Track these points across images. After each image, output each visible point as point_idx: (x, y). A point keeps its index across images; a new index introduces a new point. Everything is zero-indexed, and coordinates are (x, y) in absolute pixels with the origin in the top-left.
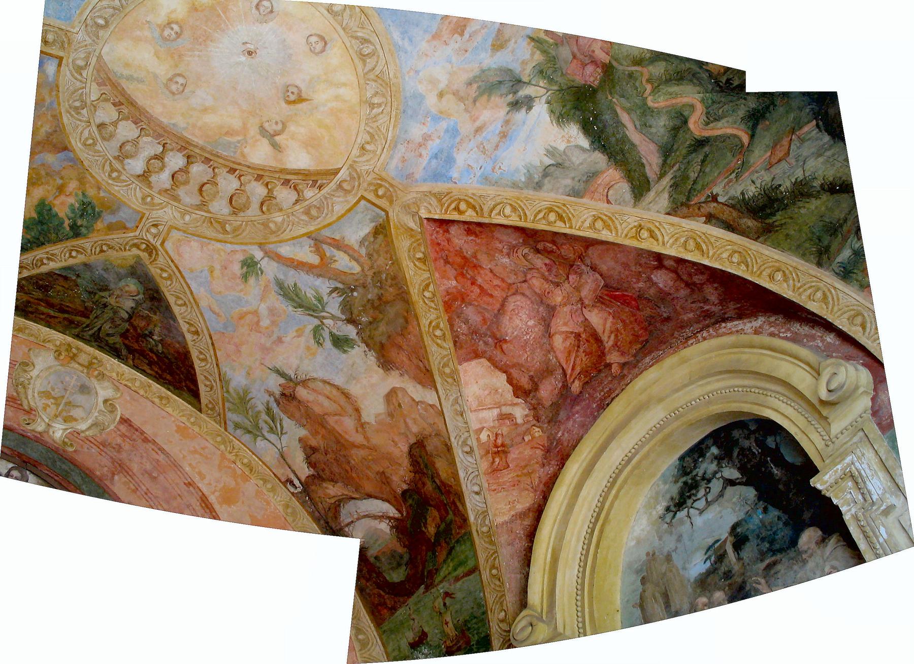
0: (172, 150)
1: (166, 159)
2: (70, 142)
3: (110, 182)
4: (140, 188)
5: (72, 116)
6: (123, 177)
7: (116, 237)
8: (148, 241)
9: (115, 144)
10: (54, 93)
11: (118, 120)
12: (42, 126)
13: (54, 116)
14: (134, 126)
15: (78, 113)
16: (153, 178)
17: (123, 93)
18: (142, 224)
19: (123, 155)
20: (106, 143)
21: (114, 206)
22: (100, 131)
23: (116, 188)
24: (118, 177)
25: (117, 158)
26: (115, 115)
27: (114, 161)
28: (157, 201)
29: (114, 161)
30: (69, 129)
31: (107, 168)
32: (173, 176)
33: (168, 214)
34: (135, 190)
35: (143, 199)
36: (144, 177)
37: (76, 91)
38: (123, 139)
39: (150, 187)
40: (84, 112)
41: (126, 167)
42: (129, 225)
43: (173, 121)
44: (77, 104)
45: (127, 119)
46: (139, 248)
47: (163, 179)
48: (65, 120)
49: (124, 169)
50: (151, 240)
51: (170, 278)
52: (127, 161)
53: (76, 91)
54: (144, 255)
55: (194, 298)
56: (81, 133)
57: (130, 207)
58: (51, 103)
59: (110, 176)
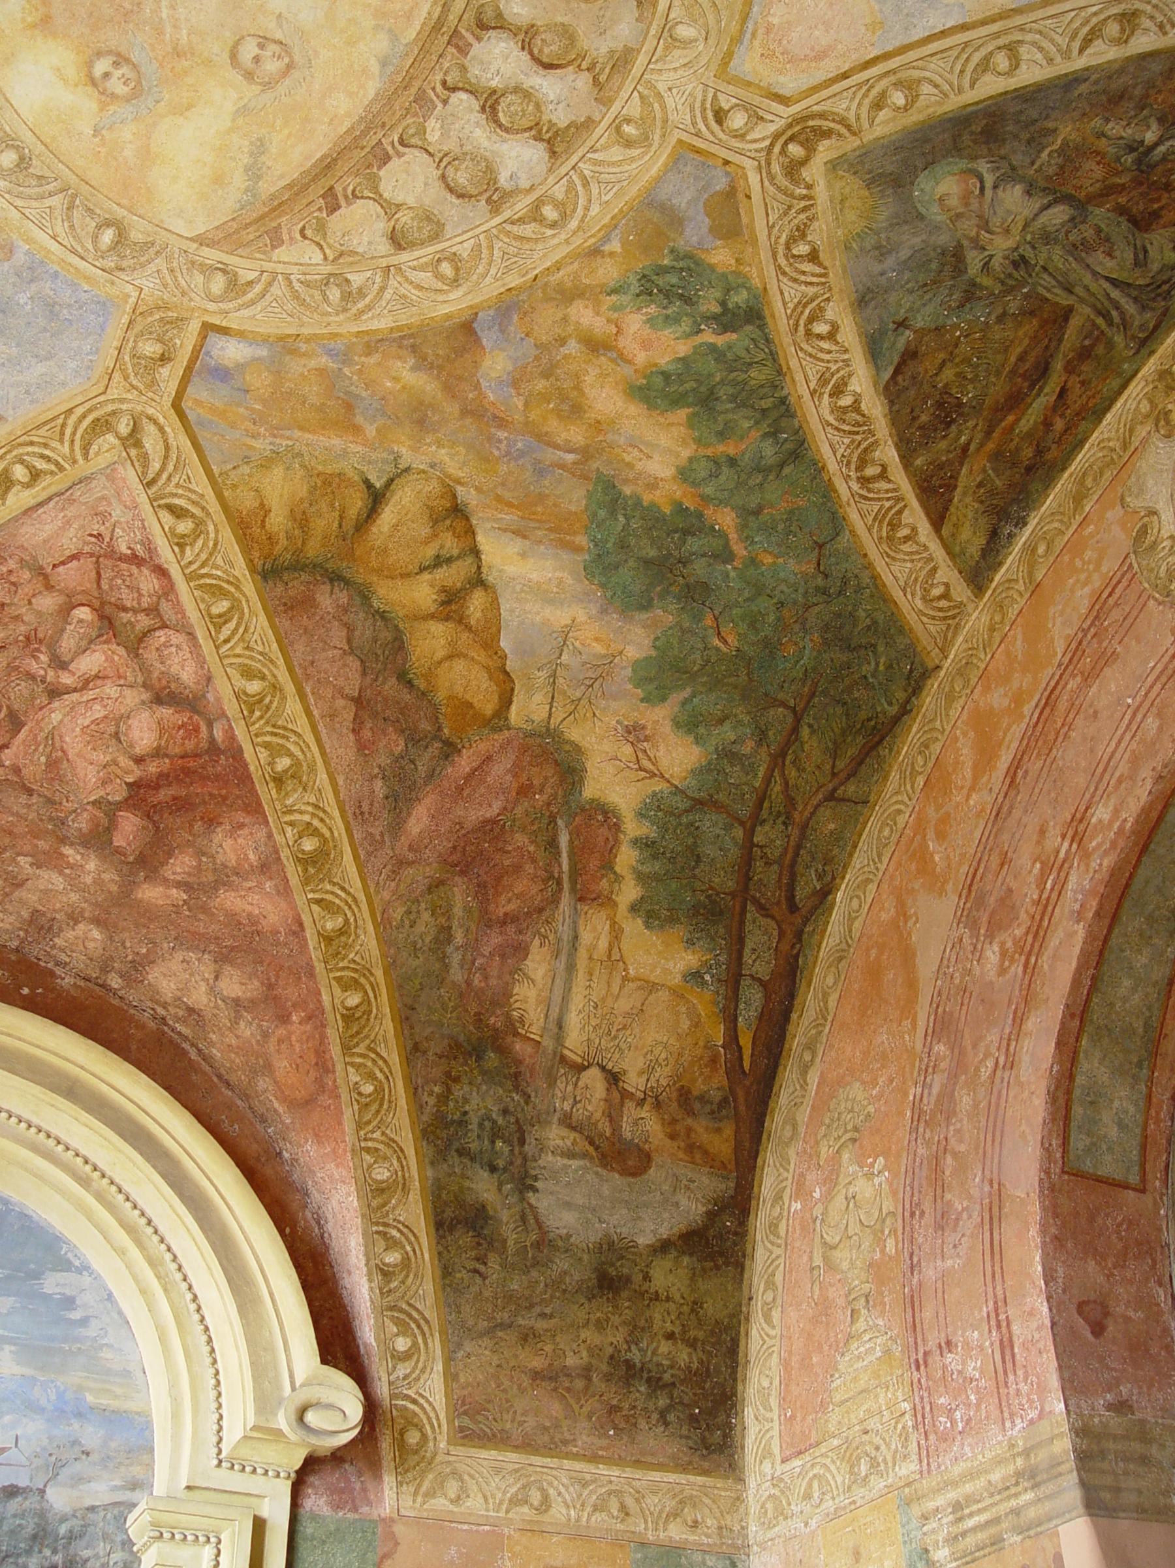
0: (464, 69)
1: (494, 84)
2: (448, 317)
3: (574, 224)
4: (592, 149)
5: (369, 308)
6: (559, 192)
7: (762, 215)
8: (776, 136)
9: (451, 210)
10: (303, 347)
11: (379, 199)
12: (396, 379)
13: (369, 349)
14: (395, 163)
15: (361, 293)
16: (561, 118)
17: (298, 189)
18: (714, 149)
19: (491, 193)
20: (449, 231)
21: (654, 217)
22: (412, 245)
23: (595, 210)
24: (557, 205)
25: (495, 207)
26: (364, 209)
27: (507, 214)
28: (634, 109)
29: (507, 214)
30: (406, 317)
31: (529, 230)
32: (549, 66)
33: (677, 85)
34: (600, 163)
35: (629, 144)
36: (555, 141)
37: (296, 296)
38: (436, 190)
39: (589, 124)
40: (357, 279)
41: (524, 184)
42: (720, 184)
43: (375, 68)
44: (334, 294)
45: (374, 183)
46: (804, 162)
47: (560, 94)
48: (375, 325)
49: (532, 188)
50: (772, 128)
51: (910, 87)
52: (503, 181)
53: (296, 296)
54: (826, 150)
55: (984, 23)
56: (419, 287)
57: (659, 180)
58: (329, 353)
59: (553, 225)
